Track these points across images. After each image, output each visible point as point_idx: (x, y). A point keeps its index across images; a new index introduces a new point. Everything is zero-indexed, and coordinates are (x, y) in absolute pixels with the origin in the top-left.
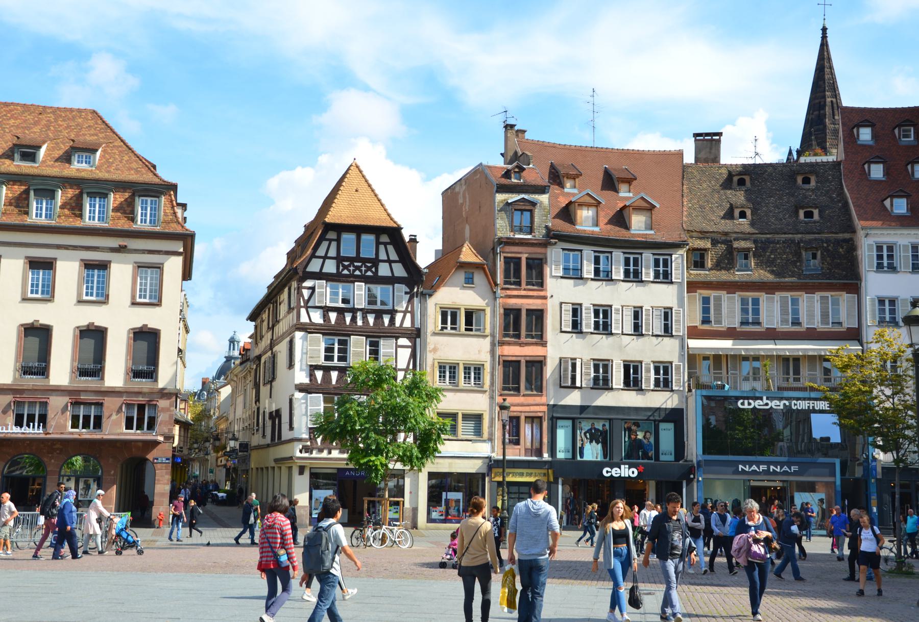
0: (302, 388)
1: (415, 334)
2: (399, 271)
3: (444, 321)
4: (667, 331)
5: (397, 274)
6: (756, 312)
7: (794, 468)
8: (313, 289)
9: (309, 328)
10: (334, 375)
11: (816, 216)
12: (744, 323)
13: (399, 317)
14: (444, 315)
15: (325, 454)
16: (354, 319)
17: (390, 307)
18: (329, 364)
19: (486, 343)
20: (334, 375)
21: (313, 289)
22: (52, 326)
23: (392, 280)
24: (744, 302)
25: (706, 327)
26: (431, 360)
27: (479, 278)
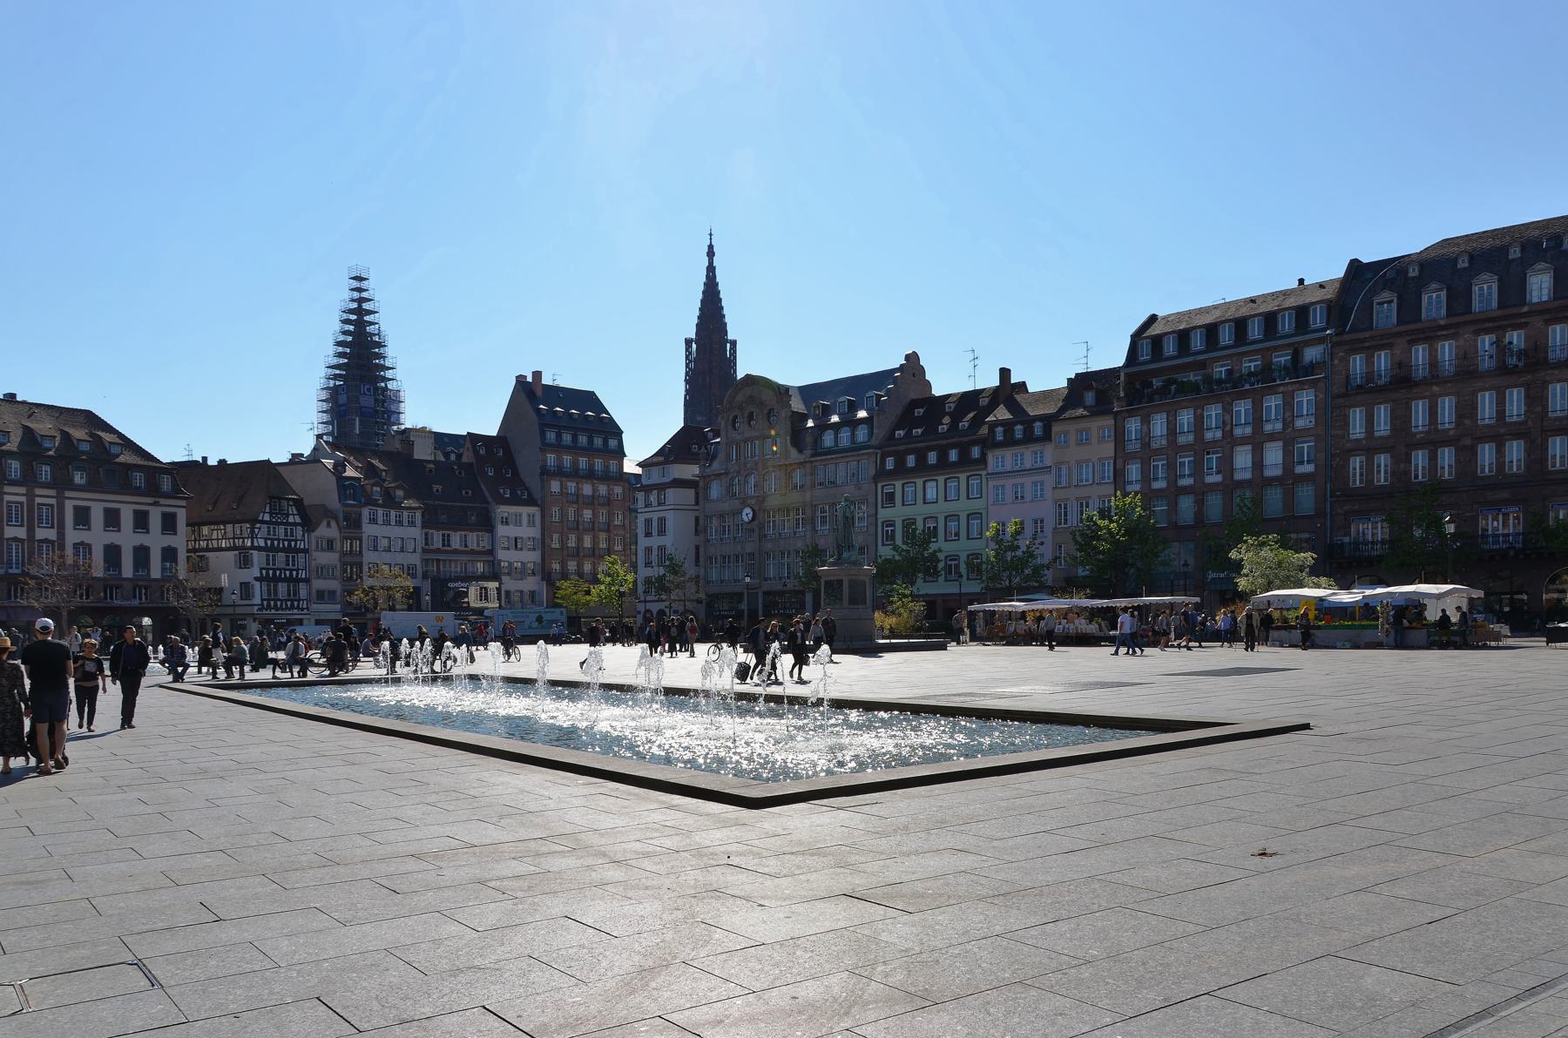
0: (256, 579)
2: (298, 519)
4: (415, 552)
5: (297, 521)
6: (449, 541)
7: (471, 613)
8: (260, 528)
9: (259, 549)
10: (271, 572)
11: (470, 494)
12: (444, 545)
13: (299, 542)
15: (268, 612)
16: (279, 544)
19: (336, 555)
20: (271, 572)
21: (260, 528)
22: (149, 548)
23: (295, 524)
24: (443, 535)
25: (427, 547)
27: (333, 523)
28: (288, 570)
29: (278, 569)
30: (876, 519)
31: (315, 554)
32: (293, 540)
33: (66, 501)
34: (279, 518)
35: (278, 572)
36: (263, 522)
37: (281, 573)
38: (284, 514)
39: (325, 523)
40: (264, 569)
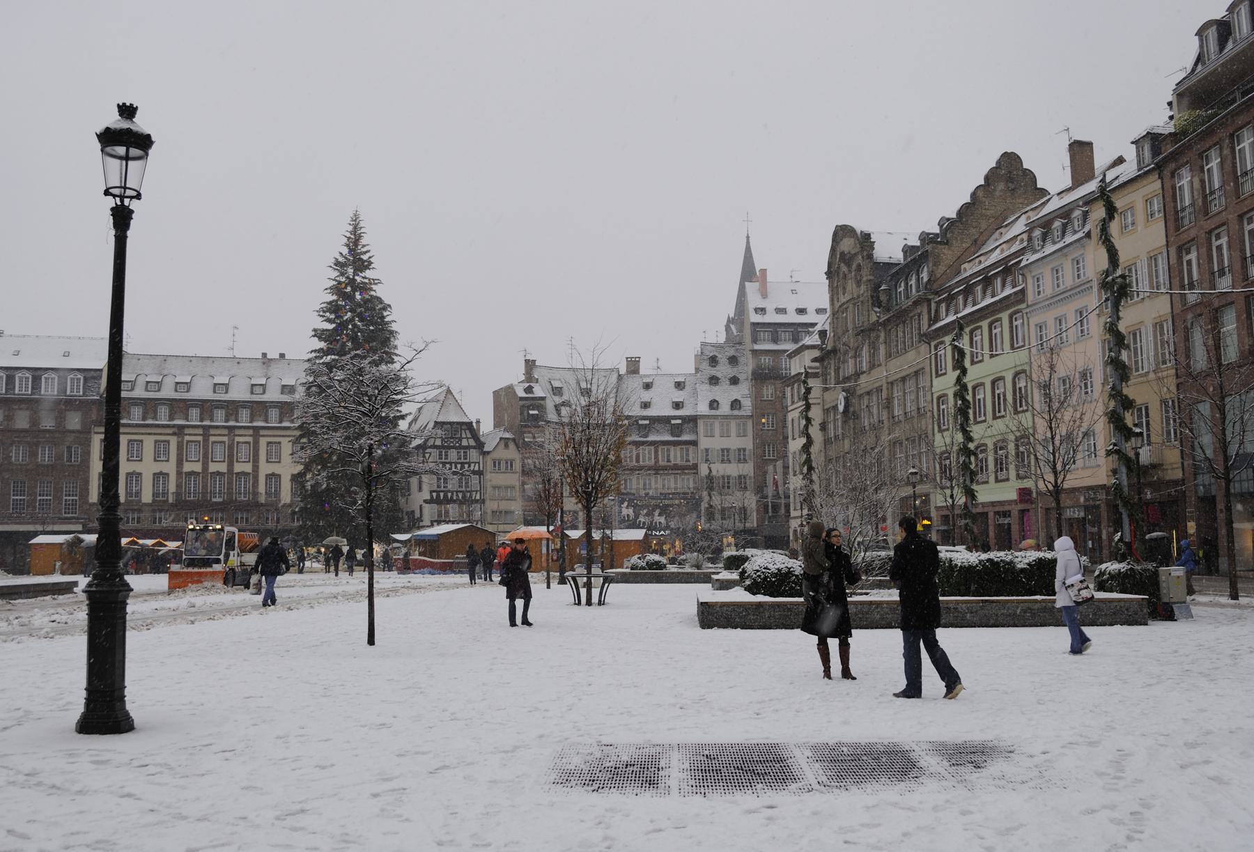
0: (426, 501)
1: (480, 473)
2: (472, 442)
3: (495, 466)
10: (442, 494)
13: (472, 465)
14: (495, 463)
17: (468, 461)
20: (442, 494)
23: (468, 447)
26: (488, 485)
28: (460, 492)
30: (932, 394)
31: (488, 476)
32: (466, 463)
33: (261, 438)
34: (452, 442)
35: (449, 495)
36: (434, 447)
37: (453, 494)
38: (456, 438)
39: (502, 445)
40: (434, 491)
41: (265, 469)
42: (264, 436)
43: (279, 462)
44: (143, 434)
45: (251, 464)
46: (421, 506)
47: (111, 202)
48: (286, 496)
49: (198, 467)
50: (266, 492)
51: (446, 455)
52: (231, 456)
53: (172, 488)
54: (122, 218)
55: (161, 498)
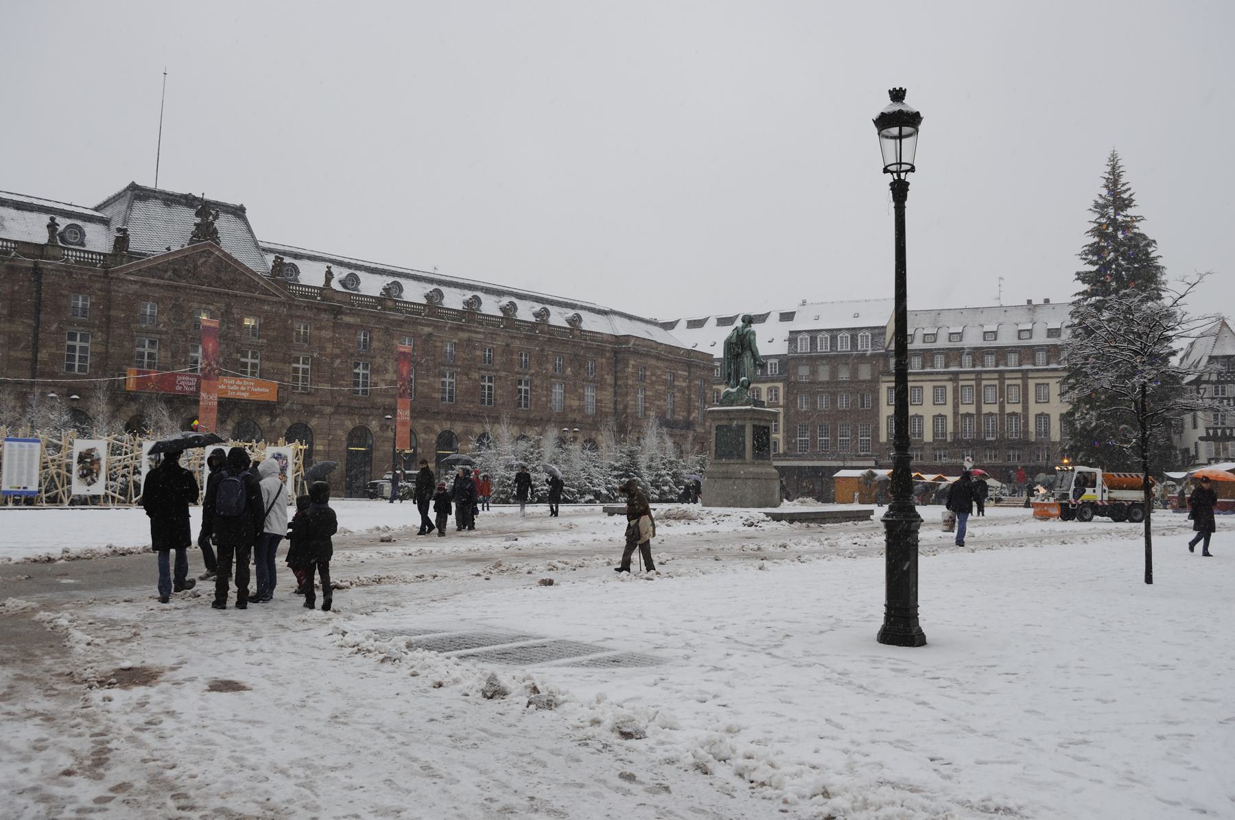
0: (1201, 439)
8: (1205, 389)
10: (1219, 432)
18: (1215, 426)
20: (1219, 432)
21: (1205, 389)
29: (1229, 428)
33: (1029, 380)
34: (1229, 376)
36: (1207, 382)
40: (1210, 428)
41: (1034, 409)
42: (1031, 378)
43: (1048, 402)
44: (922, 381)
45: (1021, 405)
46: (1196, 443)
47: (889, 178)
48: (1056, 434)
49: (972, 409)
50: (1036, 432)
51: (1223, 391)
52: (1002, 395)
53: (950, 428)
54: (900, 191)
55: (940, 438)
